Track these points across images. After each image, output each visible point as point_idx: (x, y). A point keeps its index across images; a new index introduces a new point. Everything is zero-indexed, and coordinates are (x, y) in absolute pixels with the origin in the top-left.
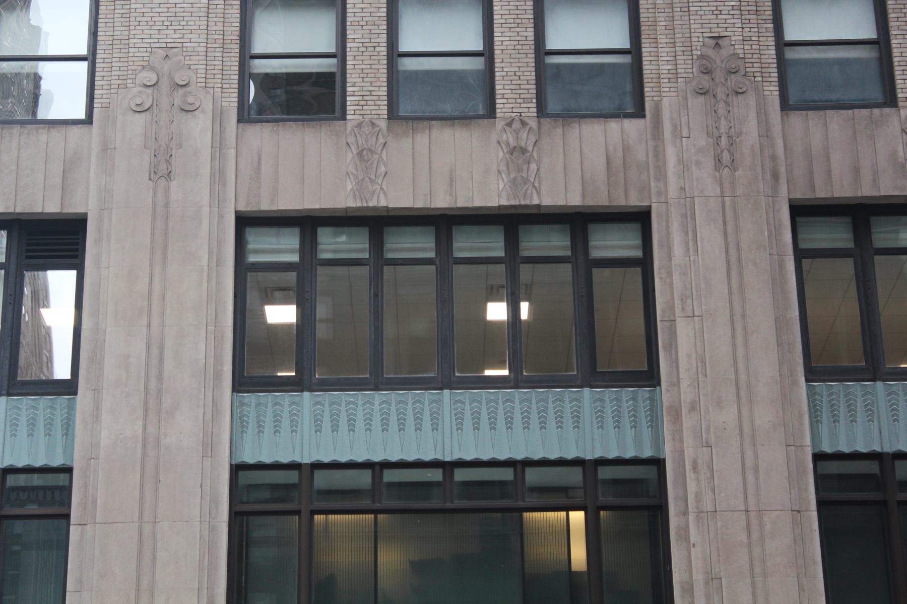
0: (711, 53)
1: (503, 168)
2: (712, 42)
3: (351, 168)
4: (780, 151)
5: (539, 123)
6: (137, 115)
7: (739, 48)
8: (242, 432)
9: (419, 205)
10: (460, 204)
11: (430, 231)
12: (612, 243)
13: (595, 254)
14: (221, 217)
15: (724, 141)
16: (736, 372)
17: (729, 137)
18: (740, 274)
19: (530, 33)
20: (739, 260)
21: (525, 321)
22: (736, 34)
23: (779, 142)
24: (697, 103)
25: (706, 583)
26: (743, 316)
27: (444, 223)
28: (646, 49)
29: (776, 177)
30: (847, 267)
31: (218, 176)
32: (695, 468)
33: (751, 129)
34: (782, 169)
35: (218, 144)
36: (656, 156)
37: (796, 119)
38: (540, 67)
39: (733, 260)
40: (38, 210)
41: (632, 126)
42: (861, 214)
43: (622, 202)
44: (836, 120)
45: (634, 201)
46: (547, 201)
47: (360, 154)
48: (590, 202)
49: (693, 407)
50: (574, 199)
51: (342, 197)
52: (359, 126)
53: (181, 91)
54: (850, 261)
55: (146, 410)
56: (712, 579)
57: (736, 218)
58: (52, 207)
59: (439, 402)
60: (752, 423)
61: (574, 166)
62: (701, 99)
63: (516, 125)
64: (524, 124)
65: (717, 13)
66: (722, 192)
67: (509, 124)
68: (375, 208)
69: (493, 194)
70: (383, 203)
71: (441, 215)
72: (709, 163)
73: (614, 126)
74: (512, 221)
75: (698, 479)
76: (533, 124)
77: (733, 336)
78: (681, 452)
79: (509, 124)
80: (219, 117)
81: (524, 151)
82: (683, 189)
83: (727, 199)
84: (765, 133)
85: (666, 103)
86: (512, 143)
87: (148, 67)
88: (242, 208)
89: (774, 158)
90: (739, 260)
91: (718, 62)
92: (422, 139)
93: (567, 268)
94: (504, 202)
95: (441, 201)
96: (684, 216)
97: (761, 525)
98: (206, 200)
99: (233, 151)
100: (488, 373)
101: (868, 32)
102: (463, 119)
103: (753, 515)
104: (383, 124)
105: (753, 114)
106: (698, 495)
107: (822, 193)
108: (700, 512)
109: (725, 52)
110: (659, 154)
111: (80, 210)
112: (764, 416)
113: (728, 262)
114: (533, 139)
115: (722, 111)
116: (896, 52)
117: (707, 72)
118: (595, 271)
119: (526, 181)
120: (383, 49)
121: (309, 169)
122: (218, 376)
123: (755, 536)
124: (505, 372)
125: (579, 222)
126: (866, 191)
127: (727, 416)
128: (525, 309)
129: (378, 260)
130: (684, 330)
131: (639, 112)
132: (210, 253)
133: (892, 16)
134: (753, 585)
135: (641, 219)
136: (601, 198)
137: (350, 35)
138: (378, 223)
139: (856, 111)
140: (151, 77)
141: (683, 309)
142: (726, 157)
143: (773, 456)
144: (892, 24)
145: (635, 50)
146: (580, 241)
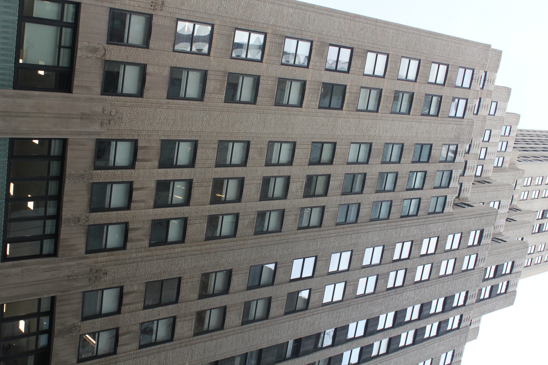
0: (102, 272)
1: (74, 216)
3: (78, 172)
4: (71, 292)
6: (102, 109)
7: (103, 279)
9: (65, 192)
10: (64, 204)
11: (54, 232)
12: (48, 246)
13: (45, 241)
14: (67, 134)
15: (76, 277)
16: (4, 286)
19: (114, 222)
20: (39, 284)
21: (27, 204)
22: (107, 278)
23: (74, 292)
24: (88, 269)
27: (59, 198)
28: (106, 253)
29: (64, 292)
30: (35, 310)
31: (80, 133)
33: (79, 284)
34: (65, 293)
35: (90, 133)
36: (73, 258)
37: (80, 295)
38: (104, 225)
40: (75, 79)
41: (83, 251)
42: (51, 313)
43: (60, 249)
44: (79, 306)
45: (60, 253)
46: (62, 229)
47: (82, 175)
48: (61, 241)
50: (62, 236)
51: (70, 169)
52: (91, 174)
53: (108, 122)
54: (42, 233)
55: (5, 112)
61: (73, 236)
62: (89, 270)
63: (87, 219)
64: (87, 221)
65: (114, 273)
67: (87, 217)
68: (65, 179)
69: (66, 213)
70: (66, 182)
73: (84, 246)
74: (57, 217)
76: (87, 224)
79: (87, 217)
80: (99, 133)
81: (79, 222)
82: (62, 267)
85: (89, 261)
86: (81, 218)
89: (69, 291)
90: (39, 284)
94: (63, 217)
95: (65, 198)
98: (72, 130)
100: (12, 185)
101: (104, 311)
102: (91, 201)
104: (91, 181)
105: (83, 284)
107: (57, 304)
111: (74, 91)
114: (82, 224)
116: (97, 320)
117: (97, 271)
118: (39, 242)
119: (69, 223)
121: (79, 160)
122: (15, 134)
124: (8, 253)
125: (55, 236)
126: (57, 316)
129: (50, 178)
130: (18, 270)
131: (87, 252)
132: (56, 131)
133: (108, 318)
135: (55, 254)
136: (61, 244)
137: (119, 171)
138: (60, 179)
140: (113, 113)
144: (105, 318)
145: (106, 250)
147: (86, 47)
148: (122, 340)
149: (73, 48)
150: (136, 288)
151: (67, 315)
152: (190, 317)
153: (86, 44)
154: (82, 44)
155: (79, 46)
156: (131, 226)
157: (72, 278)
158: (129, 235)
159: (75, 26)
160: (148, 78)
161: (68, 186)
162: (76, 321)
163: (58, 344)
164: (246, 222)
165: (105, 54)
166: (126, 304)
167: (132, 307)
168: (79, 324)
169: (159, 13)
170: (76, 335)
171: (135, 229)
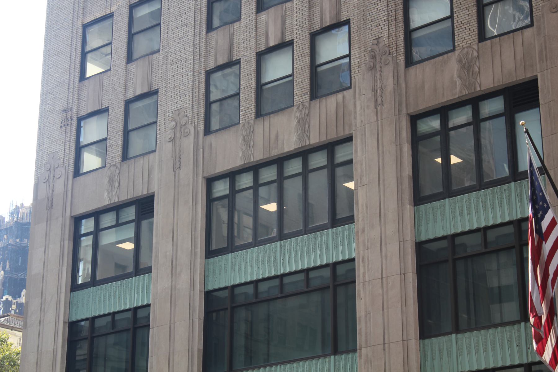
2: (376, 41)
5: (310, 104)
8: (427, 224)
17: (381, 88)
18: (383, 159)
20: (383, 152)
25: (366, 316)
26: (384, 180)
29: (400, 104)
32: (363, 261)
35: (196, 149)
39: (381, 152)
46: (312, 142)
47: (244, 139)
48: (329, 138)
49: (363, 231)
50: (324, 139)
56: (367, 313)
57: (382, 131)
58: (145, 192)
59: (444, 206)
60: (385, 234)
62: (370, 73)
66: (377, 118)
71: (506, 88)
72: (372, 105)
75: (364, 266)
76: (307, 104)
77: (379, 192)
82: (362, 121)
83: (379, 121)
84: (397, 83)
87: (174, 120)
88: (205, 175)
90: (383, 152)
91: (378, 51)
92: (267, 124)
95: (275, 152)
96: (362, 135)
97: (387, 284)
99: (201, 150)
103: (384, 279)
104: (252, 122)
105: (391, 74)
106: (364, 273)
108: (364, 282)
109: (381, 45)
112: (391, 228)
113: (378, 154)
115: (378, 77)
120: (253, 86)
123: (385, 290)
125: (330, 147)
127: (375, 233)
134: (383, 313)
136: (333, 136)
139: (437, 59)
141: (361, 182)
143: (393, 248)
149: (117, 208)
153: (106, 194)
154: (105, 201)
155: (107, 202)
156: (317, 27)
157: (379, 99)
158: (328, 24)
159: (97, 214)
160: (139, 92)
161: (258, 156)
162: (453, 58)
163: (487, 81)
165: (114, 165)
168: (457, 53)
169: (75, 111)
170: (478, 52)
171: (322, 20)
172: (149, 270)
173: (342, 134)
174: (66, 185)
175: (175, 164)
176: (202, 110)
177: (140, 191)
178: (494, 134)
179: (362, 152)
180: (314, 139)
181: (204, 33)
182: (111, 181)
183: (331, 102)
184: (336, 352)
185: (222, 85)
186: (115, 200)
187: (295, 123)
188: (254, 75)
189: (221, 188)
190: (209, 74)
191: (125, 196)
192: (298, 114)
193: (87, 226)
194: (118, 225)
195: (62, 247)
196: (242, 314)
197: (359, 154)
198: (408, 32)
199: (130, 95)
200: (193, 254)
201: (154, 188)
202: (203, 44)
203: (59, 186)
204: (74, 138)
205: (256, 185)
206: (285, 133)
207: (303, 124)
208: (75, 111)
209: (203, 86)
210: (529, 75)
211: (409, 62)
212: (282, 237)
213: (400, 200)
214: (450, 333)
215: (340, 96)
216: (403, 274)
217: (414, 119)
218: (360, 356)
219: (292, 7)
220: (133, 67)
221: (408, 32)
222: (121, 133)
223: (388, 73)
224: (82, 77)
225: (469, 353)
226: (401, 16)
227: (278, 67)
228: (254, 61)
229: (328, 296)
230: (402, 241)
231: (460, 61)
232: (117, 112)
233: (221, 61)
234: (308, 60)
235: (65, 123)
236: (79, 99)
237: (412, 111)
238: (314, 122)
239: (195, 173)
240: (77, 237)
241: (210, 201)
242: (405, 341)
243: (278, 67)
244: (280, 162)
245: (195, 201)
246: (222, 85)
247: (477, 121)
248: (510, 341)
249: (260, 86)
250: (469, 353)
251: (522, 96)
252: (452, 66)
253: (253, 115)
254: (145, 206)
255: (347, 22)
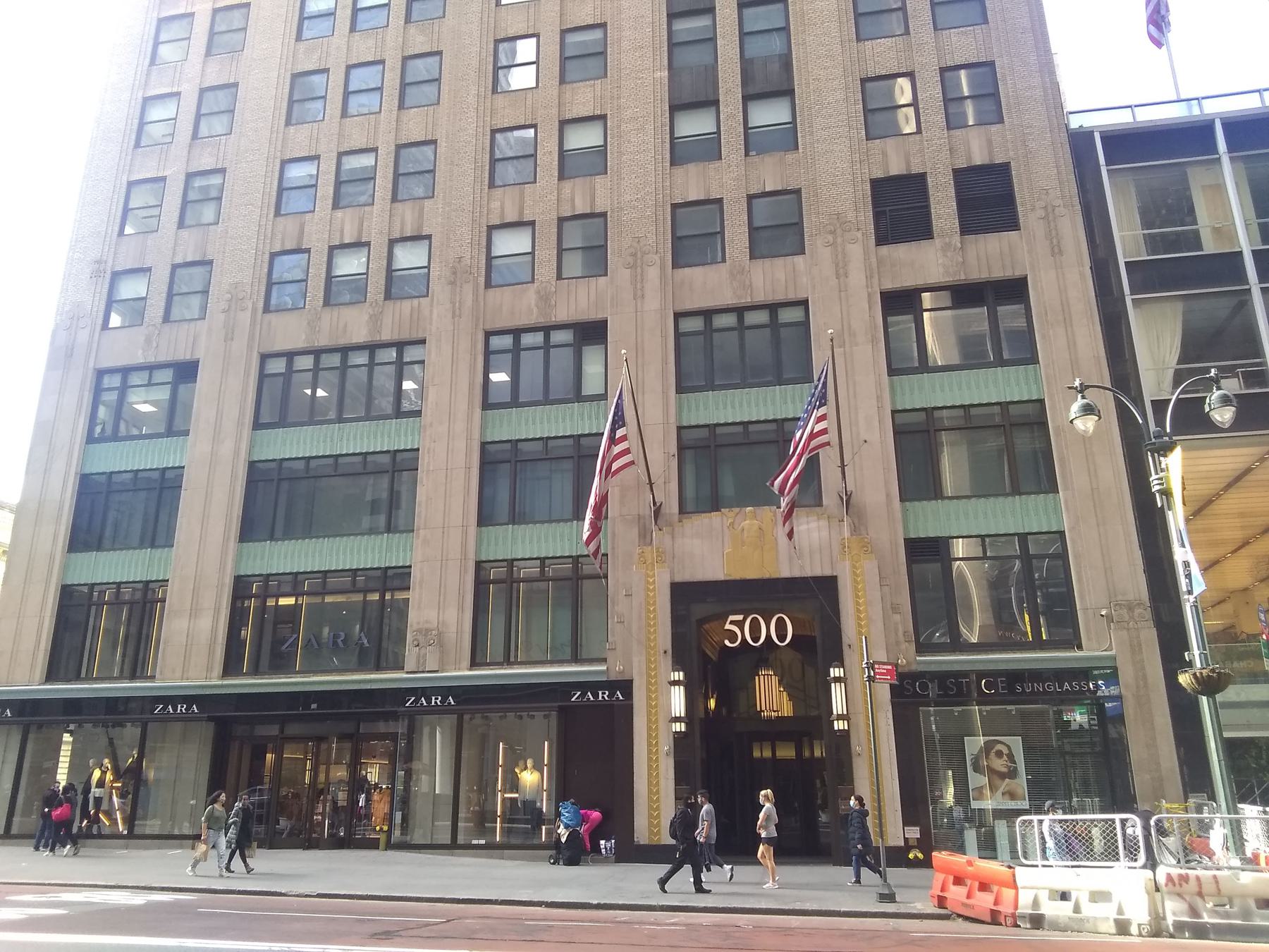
29: (478, 319)
45: (420, 336)
46: (383, 338)
49: (431, 425)
50: (396, 337)
58: (188, 357)
69: (360, 335)
72: (450, 315)
78: (424, 444)
80: (254, 310)
84: (476, 300)
87: (229, 292)
92: (335, 313)
93: (768, 330)
95: (343, 341)
110: (431, 311)
112: (460, 426)
120: (324, 275)
125: (400, 346)
128: (309, 392)
136: (405, 336)
142: (457, 312)
143: (461, 445)
146: (344, 359)
147: (144, 351)
148: (581, 207)
149: (151, 368)
150: (495, 205)
151: (519, 306)
152: (568, 95)
154: (139, 359)
156: (397, 235)
159: (126, 371)
160: (189, 259)
161: (323, 341)
162: (532, 289)
163: (562, 315)
164: (420, 39)
166: (521, 213)
167: (528, 202)
171: (402, 229)
172: (186, 433)
173: (415, 336)
174: (92, 336)
175: (227, 334)
176: (263, 289)
177: (183, 355)
178: (562, 359)
179: (436, 355)
180: (386, 336)
181: (272, 215)
182: (148, 340)
183: (406, 305)
184: (390, 529)
185: (289, 267)
186: (151, 359)
187: (366, 317)
188: (325, 266)
189: (278, 366)
190: (273, 256)
191: (162, 358)
192: (370, 311)
193: (114, 381)
194: (150, 384)
195: (81, 398)
196: (285, 486)
197: (433, 355)
198: (490, 258)
199: (179, 260)
200: (240, 423)
201: (200, 354)
202: (269, 228)
203: (83, 337)
204: (105, 290)
205: (316, 369)
206: (355, 325)
207: (375, 320)
208: (110, 264)
209: (266, 265)
210: (600, 316)
211: (488, 285)
212: (340, 420)
213: (470, 403)
214: (382, 533)
215: (416, 301)
216: (469, 468)
217: (488, 334)
218: (418, 537)
219: (372, 213)
220: (184, 233)
221: (490, 258)
222: (164, 295)
223: (468, 290)
224: (121, 232)
225: (523, 542)
226: (484, 243)
227: (350, 265)
228: (326, 251)
229: (385, 481)
230: (469, 438)
231: (538, 292)
232: (162, 275)
233: (289, 246)
234: (385, 263)
235: (97, 274)
236: (115, 254)
237: (489, 327)
238: (387, 320)
239: (250, 347)
240: (98, 390)
241: (262, 376)
242: (465, 527)
243: (350, 265)
244: (345, 351)
245: (247, 374)
246: (289, 267)
247: (547, 346)
248: (562, 536)
249: (329, 277)
250: (523, 542)
251: (592, 332)
252: (530, 295)
253: (321, 303)
254: (186, 371)
255: (429, 237)
